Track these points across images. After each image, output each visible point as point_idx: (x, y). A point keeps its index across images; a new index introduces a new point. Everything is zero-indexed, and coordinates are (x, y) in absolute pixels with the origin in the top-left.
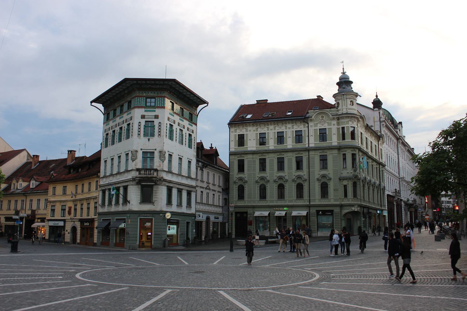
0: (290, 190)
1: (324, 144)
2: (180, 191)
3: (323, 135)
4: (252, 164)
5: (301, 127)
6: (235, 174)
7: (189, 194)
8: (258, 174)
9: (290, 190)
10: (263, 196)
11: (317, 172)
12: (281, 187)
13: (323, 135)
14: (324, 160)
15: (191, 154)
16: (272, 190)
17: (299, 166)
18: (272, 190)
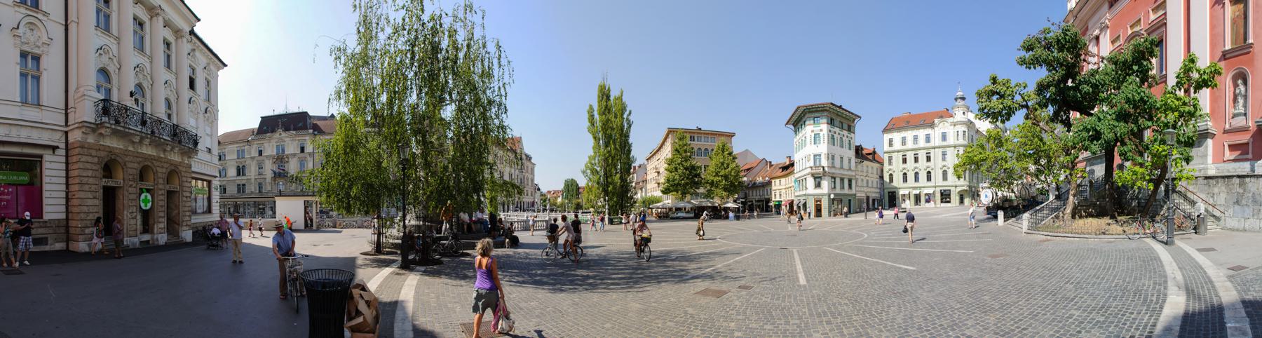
0: (923, 176)
1: (945, 143)
2: (842, 180)
3: (944, 137)
4: (897, 158)
5: (928, 131)
6: (886, 167)
7: (850, 181)
8: (902, 166)
9: (923, 176)
10: (905, 179)
11: (940, 163)
12: (917, 174)
13: (944, 137)
14: (944, 154)
15: (852, 153)
16: (911, 177)
17: (929, 159)
18: (911, 177)
